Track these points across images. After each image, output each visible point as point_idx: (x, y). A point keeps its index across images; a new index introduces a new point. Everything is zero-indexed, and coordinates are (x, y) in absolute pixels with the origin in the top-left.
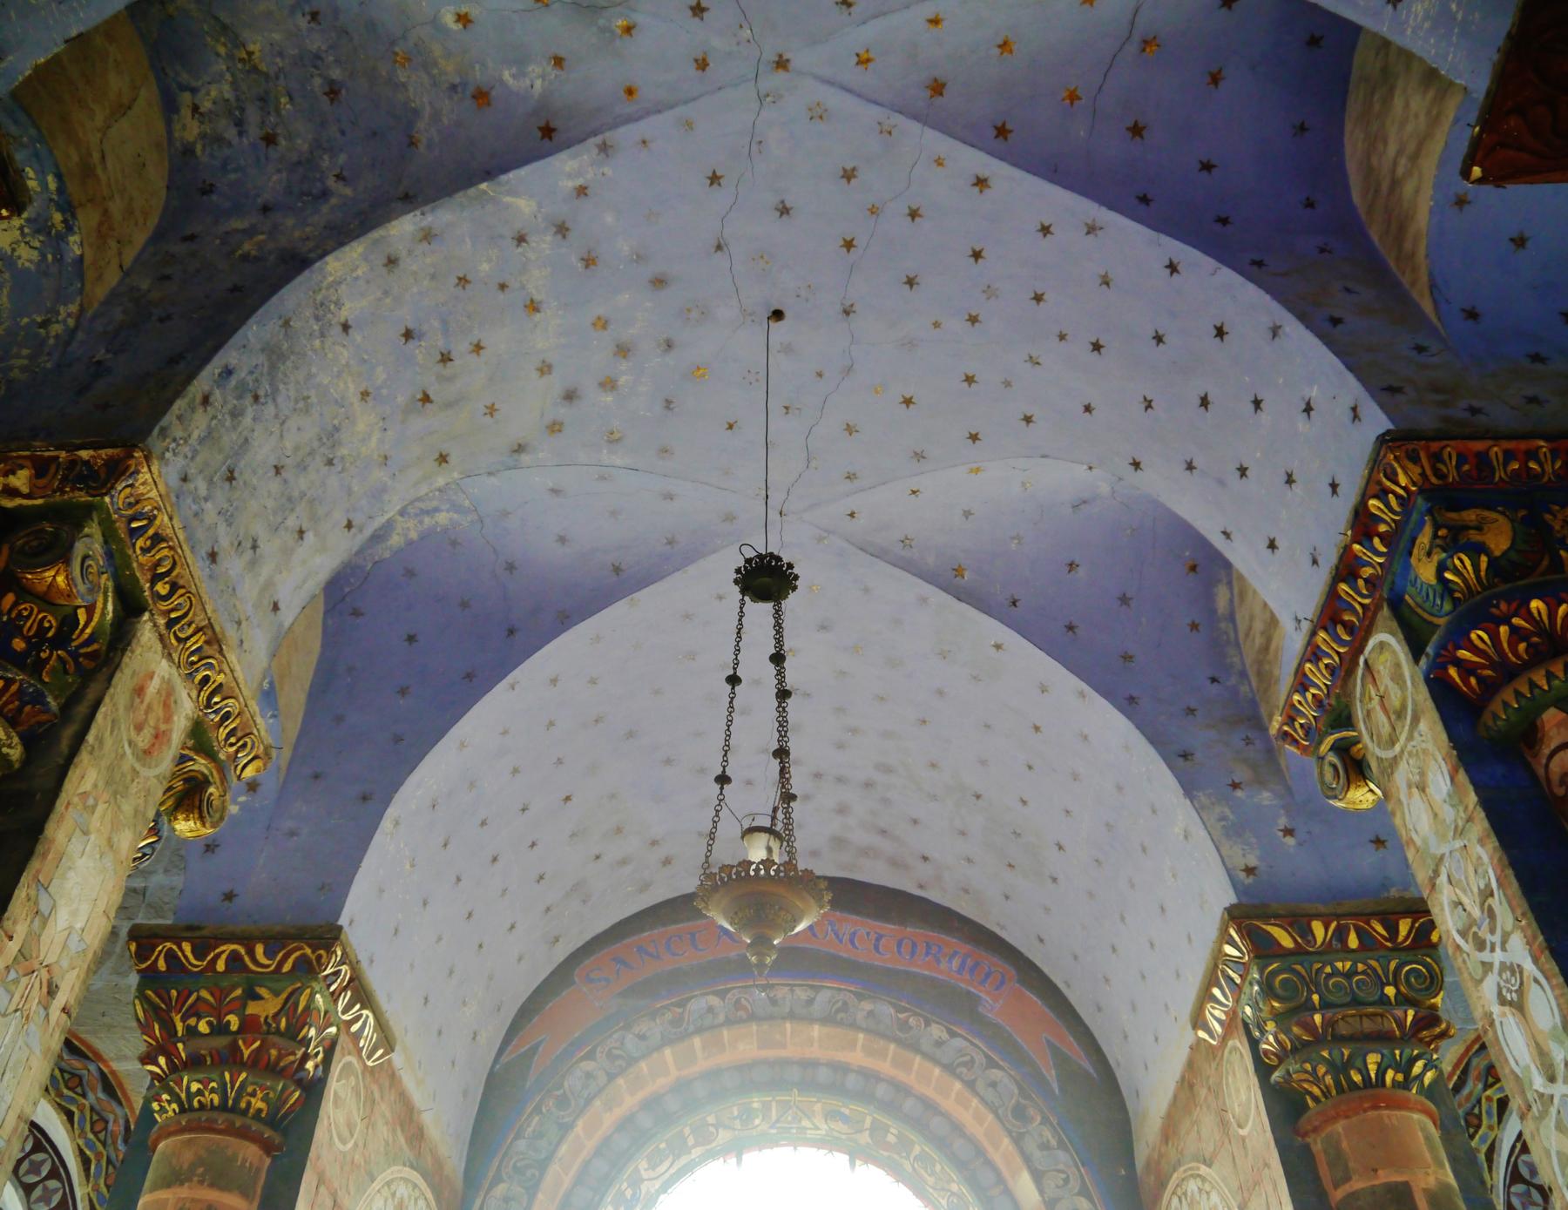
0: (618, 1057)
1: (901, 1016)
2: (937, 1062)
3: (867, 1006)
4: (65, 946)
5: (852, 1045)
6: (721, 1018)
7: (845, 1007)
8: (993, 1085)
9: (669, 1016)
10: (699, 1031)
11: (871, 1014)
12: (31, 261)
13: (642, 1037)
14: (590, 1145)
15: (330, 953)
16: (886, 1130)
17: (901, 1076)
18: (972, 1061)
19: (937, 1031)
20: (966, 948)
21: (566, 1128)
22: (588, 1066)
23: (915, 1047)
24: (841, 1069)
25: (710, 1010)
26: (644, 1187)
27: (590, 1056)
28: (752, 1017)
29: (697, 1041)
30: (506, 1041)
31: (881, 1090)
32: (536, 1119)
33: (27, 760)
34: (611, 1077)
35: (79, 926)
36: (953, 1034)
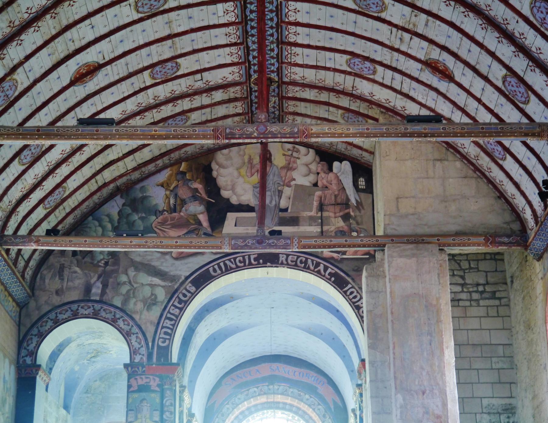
0: (234, 404)
1: (299, 393)
2: (307, 404)
3: (291, 390)
5: (288, 399)
6: (257, 394)
7: (286, 391)
8: (319, 409)
9: (245, 393)
10: (252, 397)
11: (292, 392)
13: (239, 399)
15: (193, 418)
16: (295, 417)
17: (299, 406)
18: (315, 404)
19: (307, 396)
20: (315, 375)
22: (227, 406)
23: (302, 400)
24: (285, 404)
25: (255, 392)
27: (228, 404)
28: (265, 394)
29: (252, 400)
30: (208, 400)
31: (294, 409)
32: (217, 419)
34: (233, 409)
36: (311, 397)
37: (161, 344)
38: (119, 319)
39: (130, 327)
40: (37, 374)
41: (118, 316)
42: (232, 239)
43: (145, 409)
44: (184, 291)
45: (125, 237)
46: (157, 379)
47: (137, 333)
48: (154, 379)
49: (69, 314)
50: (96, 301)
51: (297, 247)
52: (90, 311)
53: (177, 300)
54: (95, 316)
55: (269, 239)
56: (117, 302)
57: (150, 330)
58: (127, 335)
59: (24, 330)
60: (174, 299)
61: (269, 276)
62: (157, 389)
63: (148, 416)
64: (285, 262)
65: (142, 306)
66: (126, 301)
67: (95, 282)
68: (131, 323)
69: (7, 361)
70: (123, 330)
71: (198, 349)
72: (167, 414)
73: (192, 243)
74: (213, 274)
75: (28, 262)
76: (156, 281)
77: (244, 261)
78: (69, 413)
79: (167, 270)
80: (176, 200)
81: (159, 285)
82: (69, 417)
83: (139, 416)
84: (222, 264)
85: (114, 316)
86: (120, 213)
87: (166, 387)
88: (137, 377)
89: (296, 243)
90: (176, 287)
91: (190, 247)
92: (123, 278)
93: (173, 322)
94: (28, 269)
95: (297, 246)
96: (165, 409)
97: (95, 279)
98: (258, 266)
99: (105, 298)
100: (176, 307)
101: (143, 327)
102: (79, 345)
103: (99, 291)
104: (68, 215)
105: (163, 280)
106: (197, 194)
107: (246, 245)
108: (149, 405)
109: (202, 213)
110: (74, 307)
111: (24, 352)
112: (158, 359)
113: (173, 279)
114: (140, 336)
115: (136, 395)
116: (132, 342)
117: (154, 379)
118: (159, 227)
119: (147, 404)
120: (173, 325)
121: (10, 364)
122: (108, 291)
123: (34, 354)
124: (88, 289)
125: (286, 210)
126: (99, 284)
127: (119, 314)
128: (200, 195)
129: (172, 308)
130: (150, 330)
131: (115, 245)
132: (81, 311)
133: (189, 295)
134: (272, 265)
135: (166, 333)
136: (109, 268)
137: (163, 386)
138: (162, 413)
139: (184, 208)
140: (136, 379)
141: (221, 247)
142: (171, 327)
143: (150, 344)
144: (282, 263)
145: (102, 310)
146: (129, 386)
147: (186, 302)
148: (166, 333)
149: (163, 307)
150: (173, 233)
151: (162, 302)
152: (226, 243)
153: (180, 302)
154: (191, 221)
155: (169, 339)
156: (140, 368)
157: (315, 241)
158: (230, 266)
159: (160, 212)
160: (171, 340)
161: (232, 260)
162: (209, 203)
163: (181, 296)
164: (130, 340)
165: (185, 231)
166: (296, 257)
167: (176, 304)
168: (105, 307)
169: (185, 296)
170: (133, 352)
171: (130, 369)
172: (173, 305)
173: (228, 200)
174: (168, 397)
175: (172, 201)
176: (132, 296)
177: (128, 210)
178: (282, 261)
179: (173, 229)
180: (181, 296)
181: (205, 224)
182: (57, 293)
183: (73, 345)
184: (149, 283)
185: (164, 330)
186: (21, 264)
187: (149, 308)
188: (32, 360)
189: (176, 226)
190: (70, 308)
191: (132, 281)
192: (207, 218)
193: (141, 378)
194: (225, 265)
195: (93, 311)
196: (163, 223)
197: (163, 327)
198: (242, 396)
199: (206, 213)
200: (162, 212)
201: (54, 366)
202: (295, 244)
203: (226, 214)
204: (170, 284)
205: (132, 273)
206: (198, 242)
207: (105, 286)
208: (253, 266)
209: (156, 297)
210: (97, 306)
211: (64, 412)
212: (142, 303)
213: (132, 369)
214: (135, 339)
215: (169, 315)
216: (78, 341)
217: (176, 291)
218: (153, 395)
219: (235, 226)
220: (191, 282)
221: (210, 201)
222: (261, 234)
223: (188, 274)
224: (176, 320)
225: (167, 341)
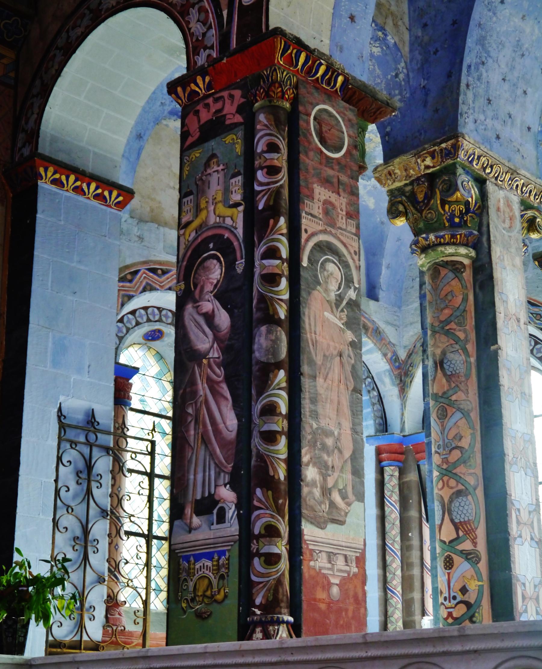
4: (516, 305)
12: (379, 52)
33: (477, 254)
35: (517, 297)
62: (239, 119)
63: (219, 197)
83: (203, 205)
108: (221, 167)
116: (190, 26)
117: (231, 97)
119: (219, 166)
164: (188, 23)
174: (261, 130)
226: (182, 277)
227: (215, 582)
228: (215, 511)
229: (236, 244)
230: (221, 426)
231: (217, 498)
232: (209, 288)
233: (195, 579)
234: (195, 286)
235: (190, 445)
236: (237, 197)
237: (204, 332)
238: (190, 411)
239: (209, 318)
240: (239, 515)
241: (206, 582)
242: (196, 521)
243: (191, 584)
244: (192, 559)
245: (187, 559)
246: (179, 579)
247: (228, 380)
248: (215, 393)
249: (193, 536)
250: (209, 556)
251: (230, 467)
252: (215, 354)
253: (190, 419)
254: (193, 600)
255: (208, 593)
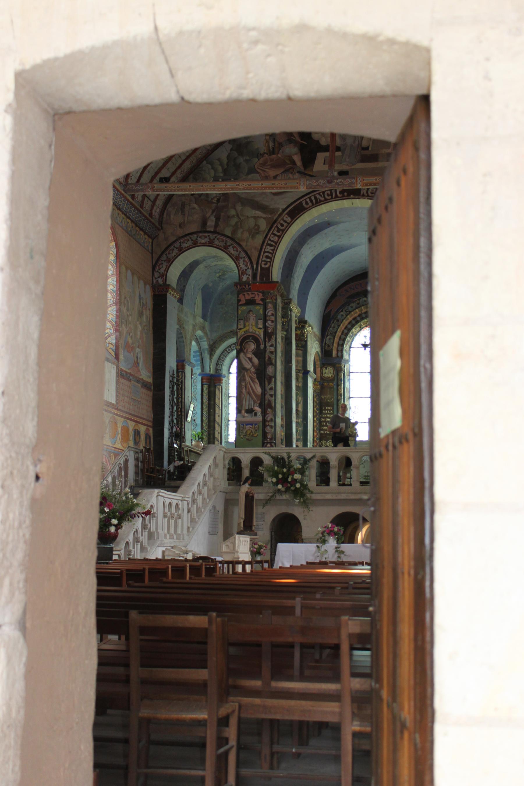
0: (348, 311)
10: (363, 305)
14: (344, 328)
15: (306, 324)
21: (339, 326)
22: (342, 313)
26: (354, 333)
27: (342, 311)
32: (333, 324)
33: (287, 334)
34: (347, 316)
37: (263, 266)
38: (229, 246)
39: (238, 253)
40: (168, 291)
41: (228, 244)
42: (307, 181)
43: (251, 318)
44: (282, 222)
45: (221, 181)
46: (261, 295)
47: (244, 258)
48: (258, 295)
49: (190, 243)
50: (210, 232)
51: (361, 185)
52: (190, 243)
53: (276, 229)
54: (211, 244)
55: (337, 179)
56: (228, 232)
57: (254, 255)
58: (236, 259)
59: (156, 257)
60: (273, 228)
61: (354, 205)
62: (261, 302)
63: (254, 324)
64: (366, 194)
65: (248, 235)
66: (234, 232)
67: (209, 217)
68: (239, 249)
69: (142, 282)
70: (233, 255)
71: (305, 267)
72: (269, 322)
73: (274, 184)
74: (306, 206)
75: (154, 202)
76: (259, 213)
77: (332, 195)
78: (207, 321)
79: (267, 204)
80: (274, 144)
81: (261, 217)
82: (207, 324)
83: (247, 324)
84: (313, 198)
85: (226, 243)
86: (228, 157)
87: (268, 300)
88: (245, 293)
89: (359, 181)
90: (275, 218)
91: (273, 188)
92: (232, 212)
93: (273, 248)
94: (155, 208)
95: (360, 184)
96: (268, 318)
97: (210, 213)
98: (343, 198)
99: (218, 230)
100: (275, 235)
101: (249, 252)
102: (206, 267)
103: (214, 224)
104: (184, 161)
105: (264, 213)
106: (292, 137)
107: (318, 185)
109: (296, 154)
110: (194, 237)
111: (156, 275)
112: (261, 278)
113: (273, 211)
114: (247, 259)
115: (244, 308)
116: (240, 264)
117: (258, 295)
118: (261, 168)
119: (253, 314)
120: (273, 250)
121: (145, 283)
122: (220, 223)
123: (164, 276)
124: (204, 223)
125: (367, 148)
126: (213, 218)
127: (229, 242)
128: (294, 138)
129: (272, 236)
130: (254, 255)
131: (213, 189)
132: (200, 241)
133: (285, 224)
134: (354, 197)
135: (267, 257)
136: (220, 204)
137: (265, 300)
138: (265, 321)
139: (281, 151)
140: (244, 295)
141: (298, 187)
142: (271, 252)
143: (255, 266)
144: (363, 195)
145: (216, 239)
146: (239, 301)
147: (283, 231)
148: (267, 257)
149: (265, 235)
150: (272, 173)
151: (264, 231)
152: (302, 184)
153: (278, 231)
154: (287, 161)
155: (270, 262)
156: (247, 286)
157: (375, 179)
158: (319, 199)
159: (261, 154)
160: (272, 262)
161: (321, 194)
162: (302, 145)
163: (279, 226)
164: (239, 263)
165: (282, 170)
166: (375, 189)
167: (275, 232)
168: (218, 237)
169: (282, 225)
170: (242, 273)
171: (239, 287)
172: (273, 233)
173: (318, 142)
174: (269, 309)
175: (271, 145)
176: (239, 227)
177: (235, 154)
178: (363, 193)
179: (272, 169)
180: (279, 226)
181: (299, 163)
182: (181, 226)
183: (201, 266)
184: (253, 215)
185: (266, 254)
186: (147, 205)
187: (253, 237)
188: (163, 281)
189: (274, 166)
190: (191, 238)
191: (239, 214)
192: (300, 158)
193: (248, 294)
194: (316, 198)
195: (209, 240)
196: (264, 164)
197: (265, 252)
198: (354, 305)
199: (299, 154)
200: (262, 155)
201: (187, 284)
202: (358, 182)
203: (316, 154)
204: (270, 216)
205: (239, 207)
206: (279, 184)
207: (218, 219)
208: (339, 199)
209: (259, 227)
210: (212, 236)
211: (202, 320)
212: (248, 233)
213: (240, 286)
214: (243, 263)
215: (270, 242)
216: (205, 263)
217: (275, 222)
218: (257, 307)
219: (324, 164)
220: (287, 214)
221: (303, 143)
222: (330, 175)
223: (284, 207)
224: (275, 246)
225: (268, 264)
226: (239, 344)
227: (253, 431)
228: (253, 413)
229: (260, 340)
230: (255, 390)
231: (254, 409)
232: (250, 350)
233: (246, 430)
234: (245, 348)
235: (243, 394)
236: (261, 326)
237: (249, 364)
238: (243, 384)
239: (250, 359)
240: (262, 415)
241: (250, 431)
242: (246, 415)
243: (245, 432)
244: (245, 425)
245: (243, 425)
246: (240, 430)
247: (258, 378)
248: (253, 381)
249: (245, 419)
250: (252, 425)
251: (259, 402)
252: (253, 370)
253: (243, 386)
254: (245, 435)
255: (251, 434)
